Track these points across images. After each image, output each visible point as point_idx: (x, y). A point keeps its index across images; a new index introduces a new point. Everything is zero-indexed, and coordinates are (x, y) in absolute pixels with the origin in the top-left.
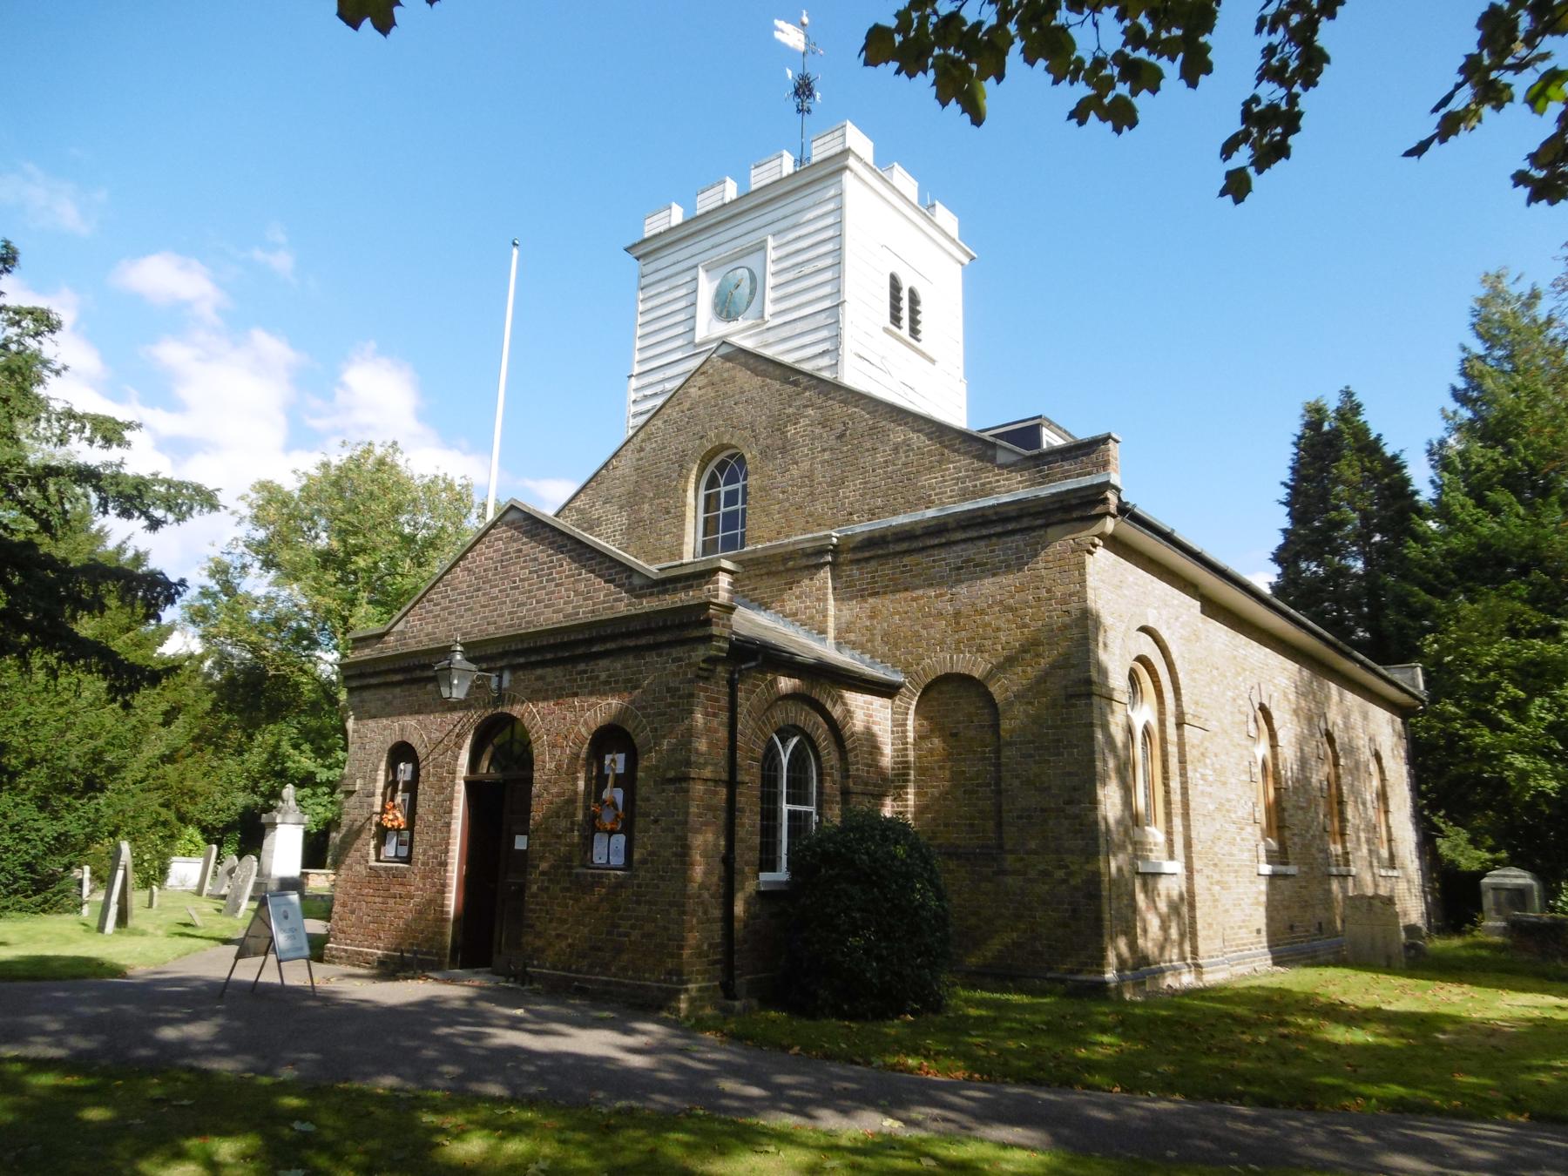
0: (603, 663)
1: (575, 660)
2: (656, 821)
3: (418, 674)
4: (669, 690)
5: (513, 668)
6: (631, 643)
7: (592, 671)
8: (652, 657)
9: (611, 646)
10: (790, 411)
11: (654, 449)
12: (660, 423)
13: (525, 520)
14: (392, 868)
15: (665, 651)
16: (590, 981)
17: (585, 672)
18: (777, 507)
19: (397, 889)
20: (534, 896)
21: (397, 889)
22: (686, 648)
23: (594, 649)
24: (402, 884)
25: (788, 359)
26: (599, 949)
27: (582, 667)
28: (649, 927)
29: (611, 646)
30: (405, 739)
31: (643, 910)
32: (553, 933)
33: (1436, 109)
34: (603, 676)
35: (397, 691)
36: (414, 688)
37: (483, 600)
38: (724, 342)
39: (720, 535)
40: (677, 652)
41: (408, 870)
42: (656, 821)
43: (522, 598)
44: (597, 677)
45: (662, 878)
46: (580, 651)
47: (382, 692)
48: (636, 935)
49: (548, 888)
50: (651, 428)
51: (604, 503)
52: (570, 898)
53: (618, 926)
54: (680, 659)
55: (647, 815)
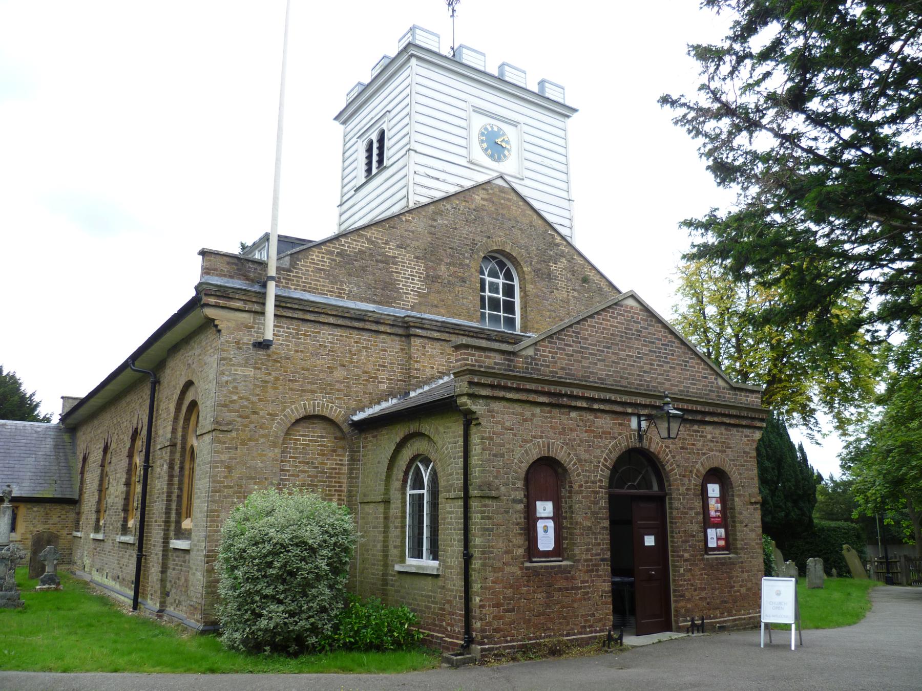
0: (709, 428)
1: (693, 422)
2: (746, 526)
3: (565, 400)
4: (745, 452)
5: (649, 417)
6: (727, 421)
7: (702, 432)
8: (734, 431)
9: (716, 419)
10: (550, 252)
11: (446, 226)
12: (449, 207)
13: (641, 310)
14: (553, 567)
15: (740, 429)
16: (725, 621)
17: (698, 432)
18: (548, 313)
19: (562, 584)
20: (683, 575)
21: (562, 584)
22: (751, 431)
23: (707, 419)
24: (567, 579)
25: (550, 218)
26: (726, 602)
27: (696, 427)
28: (749, 584)
29: (716, 419)
30: (552, 454)
31: (745, 575)
32: (697, 598)
33: (343, 117)
34: (709, 437)
35: (538, 410)
36: (556, 412)
37: (614, 358)
38: (501, 177)
39: (502, 314)
40: (747, 431)
41: (572, 566)
42: (746, 526)
43: (647, 368)
44: (706, 437)
45: (752, 557)
46: (699, 418)
47: (518, 408)
48: (743, 590)
49: (690, 570)
50: (441, 206)
51: (398, 247)
52: (705, 574)
53: (734, 587)
54: (748, 436)
55: (741, 522)
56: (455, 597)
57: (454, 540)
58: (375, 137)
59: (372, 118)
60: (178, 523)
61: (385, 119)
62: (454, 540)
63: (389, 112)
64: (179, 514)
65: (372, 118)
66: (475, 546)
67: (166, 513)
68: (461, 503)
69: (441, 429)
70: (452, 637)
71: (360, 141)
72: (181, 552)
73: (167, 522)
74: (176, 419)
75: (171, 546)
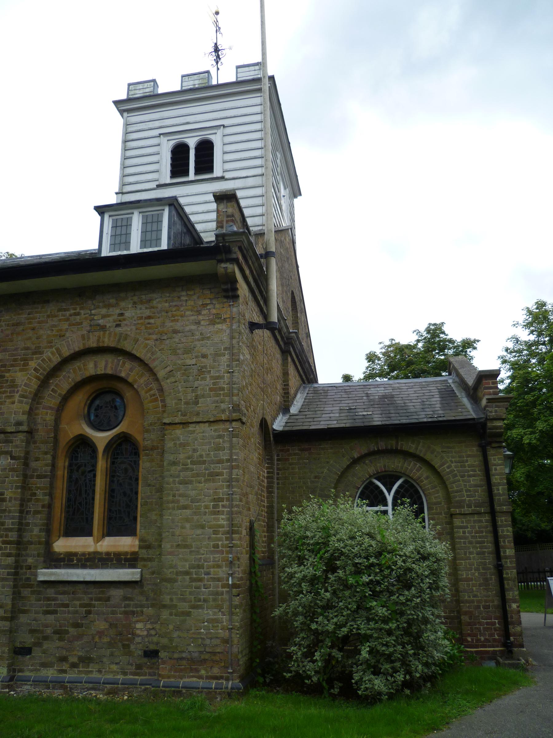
56: (478, 607)
57: (471, 553)
58: (192, 143)
59: (188, 123)
60: (48, 544)
61: (220, 132)
62: (471, 553)
63: (224, 126)
64: (48, 530)
65: (188, 123)
66: (507, 557)
67: (19, 530)
68: (487, 517)
69: (438, 449)
70: (477, 647)
71: (164, 140)
72: (81, 586)
73: (20, 544)
74: (37, 397)
75: (41, 578)
